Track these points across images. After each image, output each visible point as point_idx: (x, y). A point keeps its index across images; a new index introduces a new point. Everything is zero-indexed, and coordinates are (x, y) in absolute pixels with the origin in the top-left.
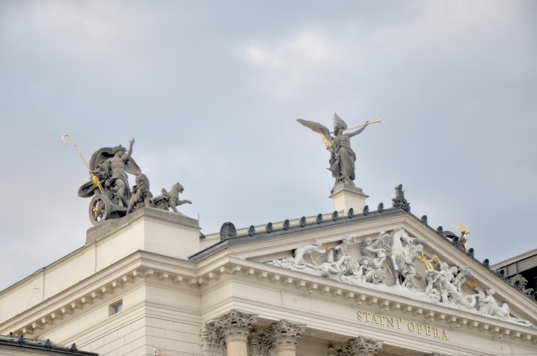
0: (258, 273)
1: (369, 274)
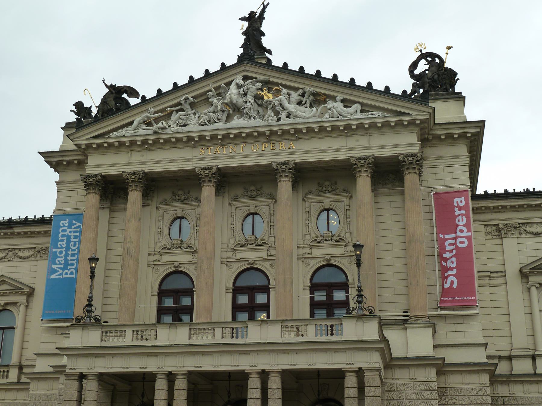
0: (100, 146)
1: (202, 120)
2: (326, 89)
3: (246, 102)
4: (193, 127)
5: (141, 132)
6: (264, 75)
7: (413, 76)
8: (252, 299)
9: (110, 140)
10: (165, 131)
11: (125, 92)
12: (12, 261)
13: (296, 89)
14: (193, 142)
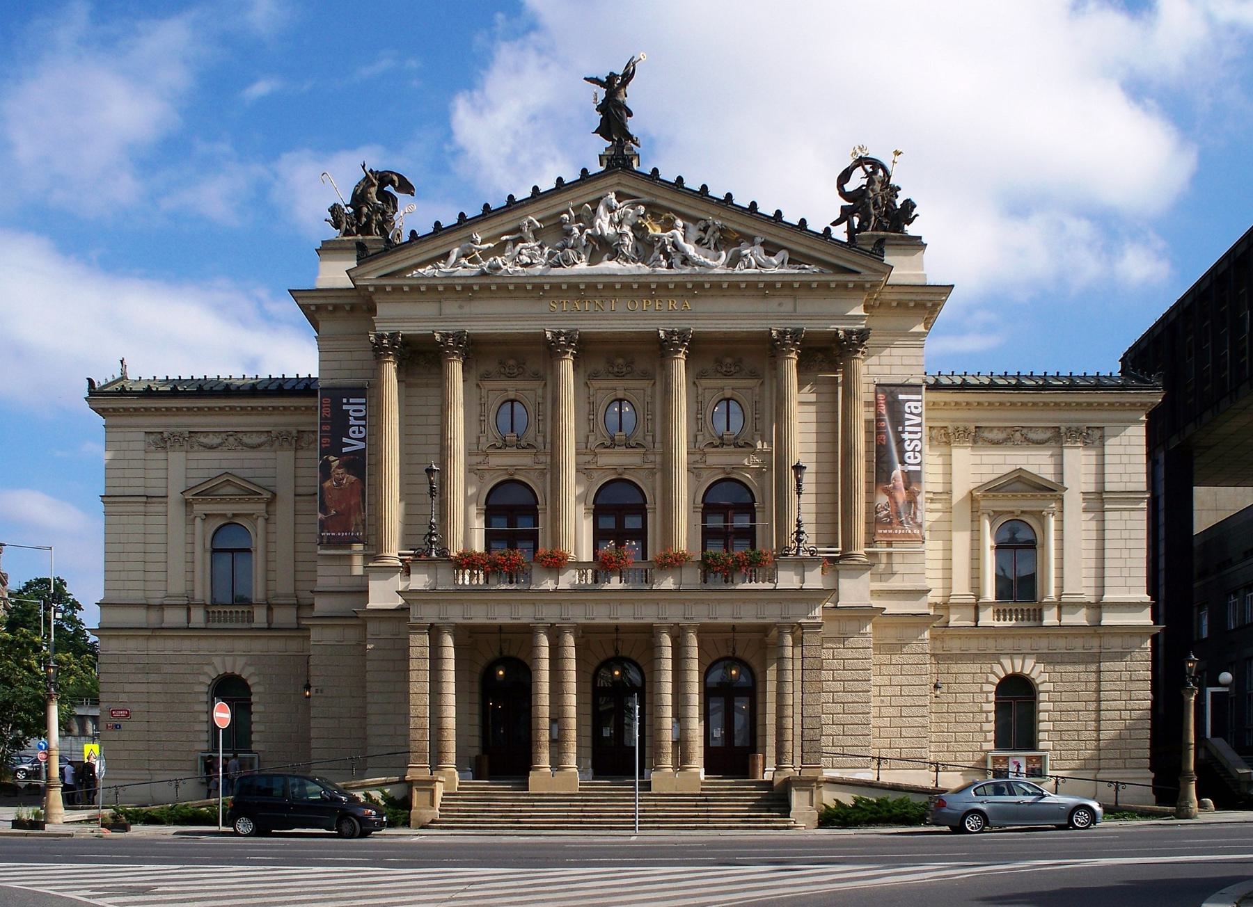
0: (397, 289)
1: (554, 259)
5: (460, 271)
6: (647, 193)
7: (843, 194)
8: (620, 523)
13: (695, 220)
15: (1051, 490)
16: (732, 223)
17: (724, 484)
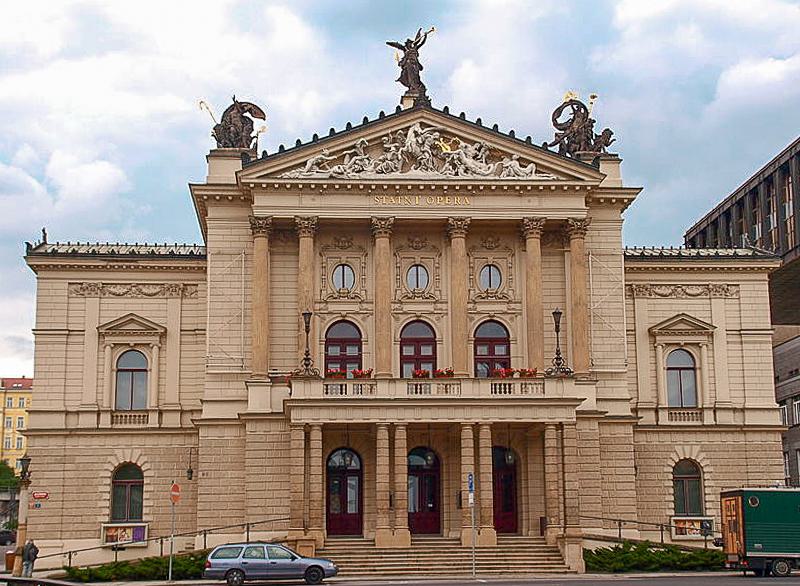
1: (379, 167)
2: (504, 146)
3: (423, 152)
4: (369, 174)
5: (316, 175)
8: (418, 351)
9: (282, 181)
10: (341, 176)
11: (250, 111)
12: (136, 298)
13: (473, 143)
14: (367, 190)
15: (704, 329)
16: (497, 143)
17: (488, 324)
